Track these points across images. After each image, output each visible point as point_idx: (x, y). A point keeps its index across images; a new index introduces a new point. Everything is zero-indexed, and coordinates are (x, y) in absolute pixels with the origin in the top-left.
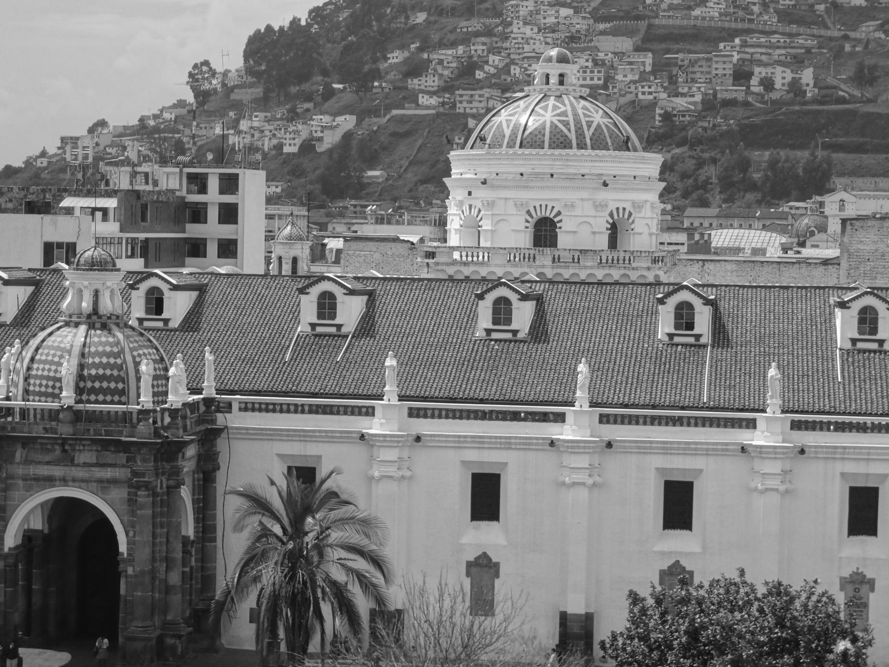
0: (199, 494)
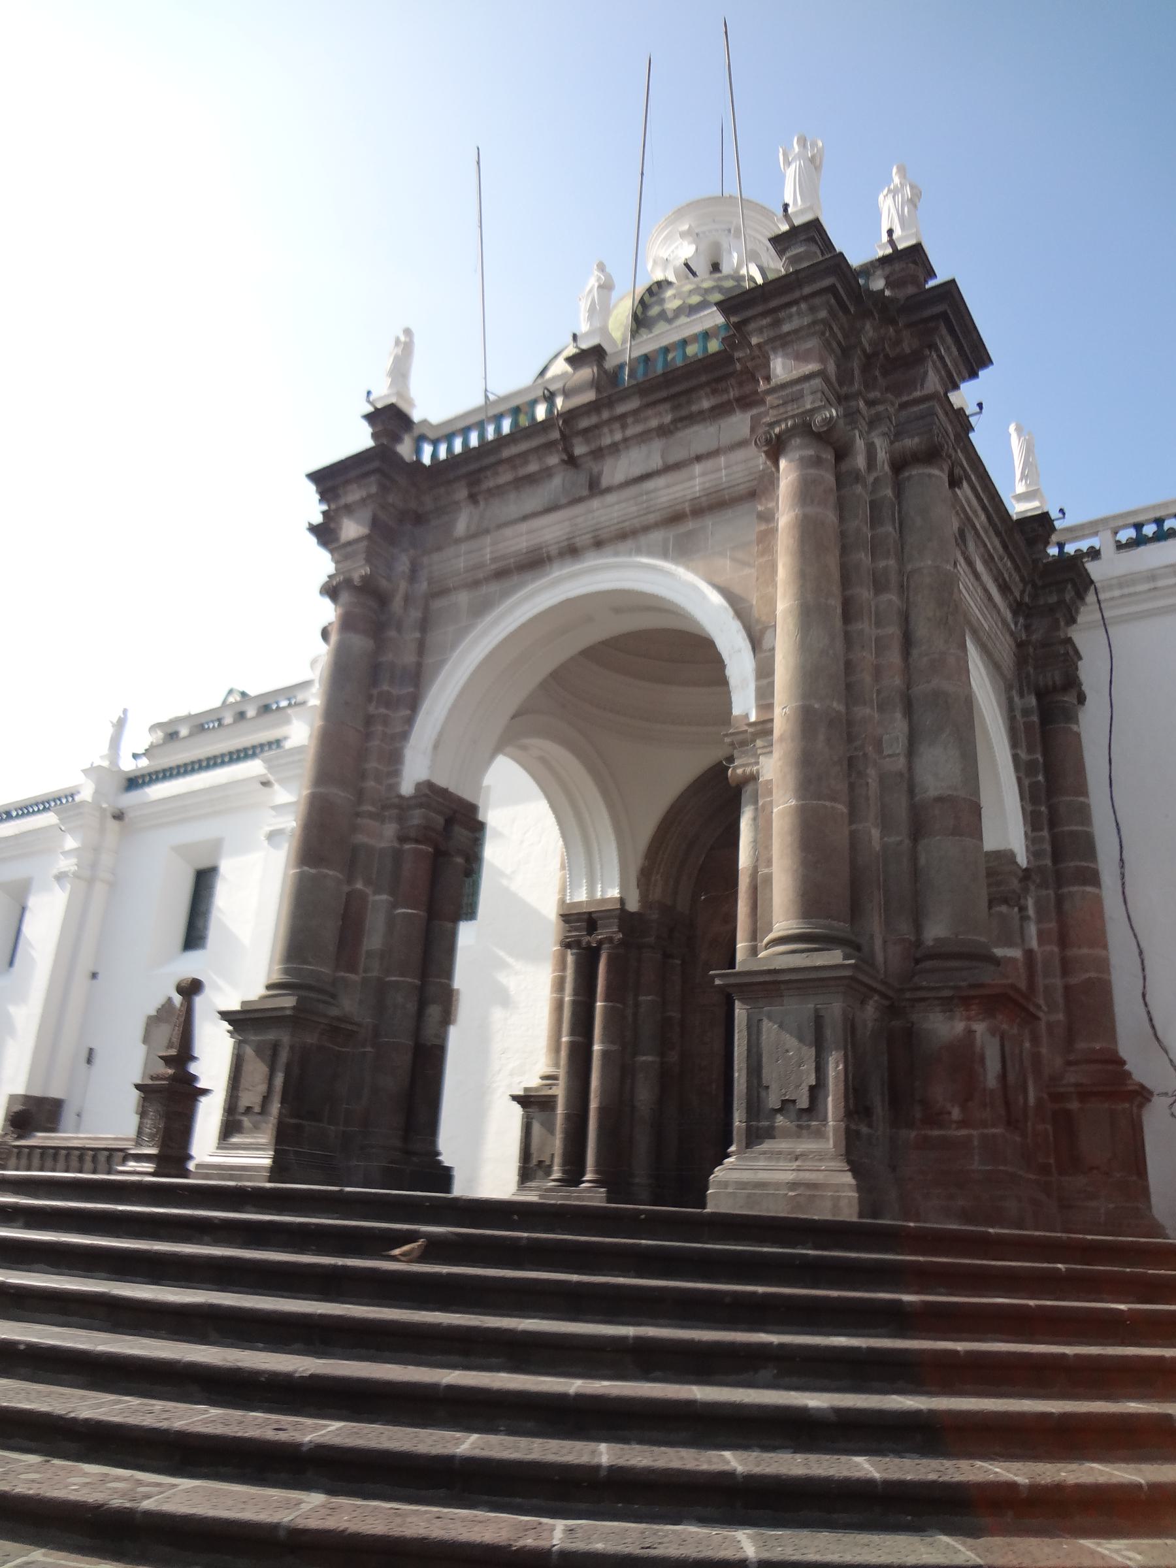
0: (1030, 750)
